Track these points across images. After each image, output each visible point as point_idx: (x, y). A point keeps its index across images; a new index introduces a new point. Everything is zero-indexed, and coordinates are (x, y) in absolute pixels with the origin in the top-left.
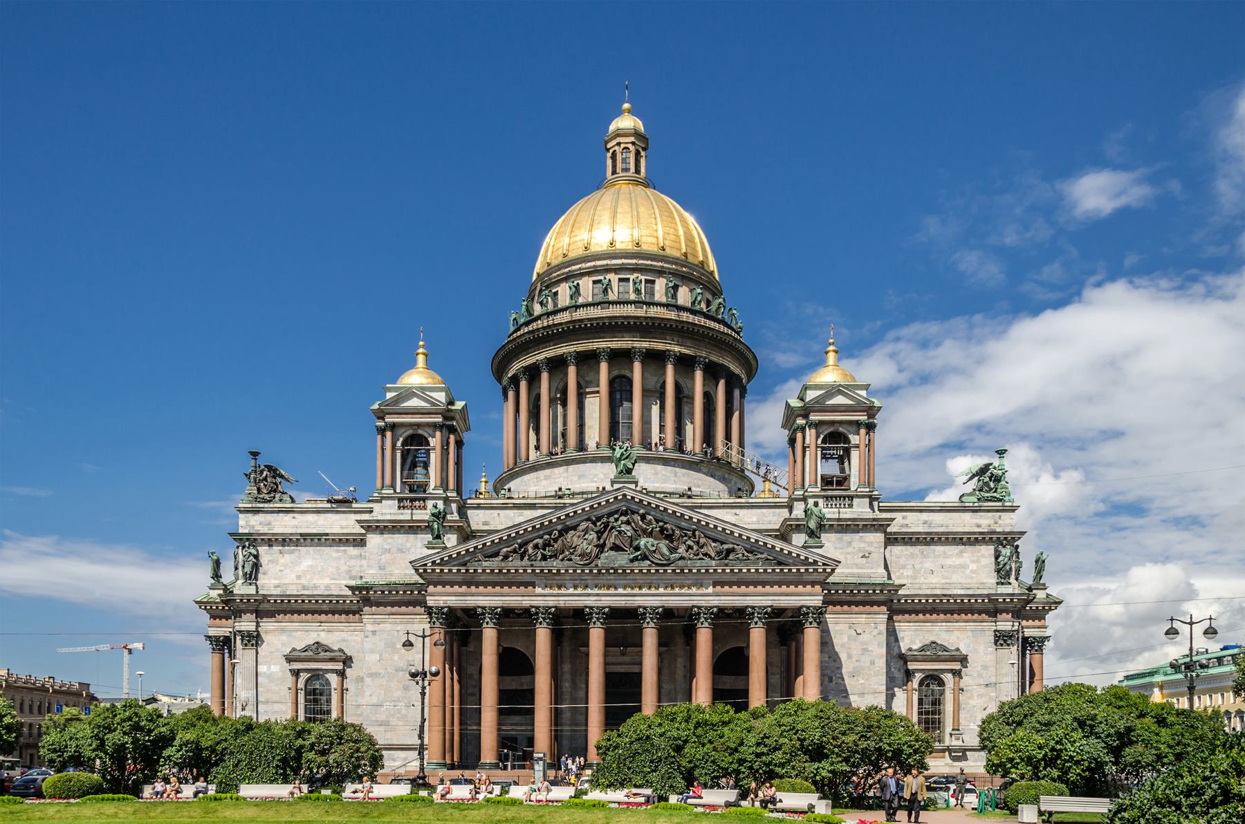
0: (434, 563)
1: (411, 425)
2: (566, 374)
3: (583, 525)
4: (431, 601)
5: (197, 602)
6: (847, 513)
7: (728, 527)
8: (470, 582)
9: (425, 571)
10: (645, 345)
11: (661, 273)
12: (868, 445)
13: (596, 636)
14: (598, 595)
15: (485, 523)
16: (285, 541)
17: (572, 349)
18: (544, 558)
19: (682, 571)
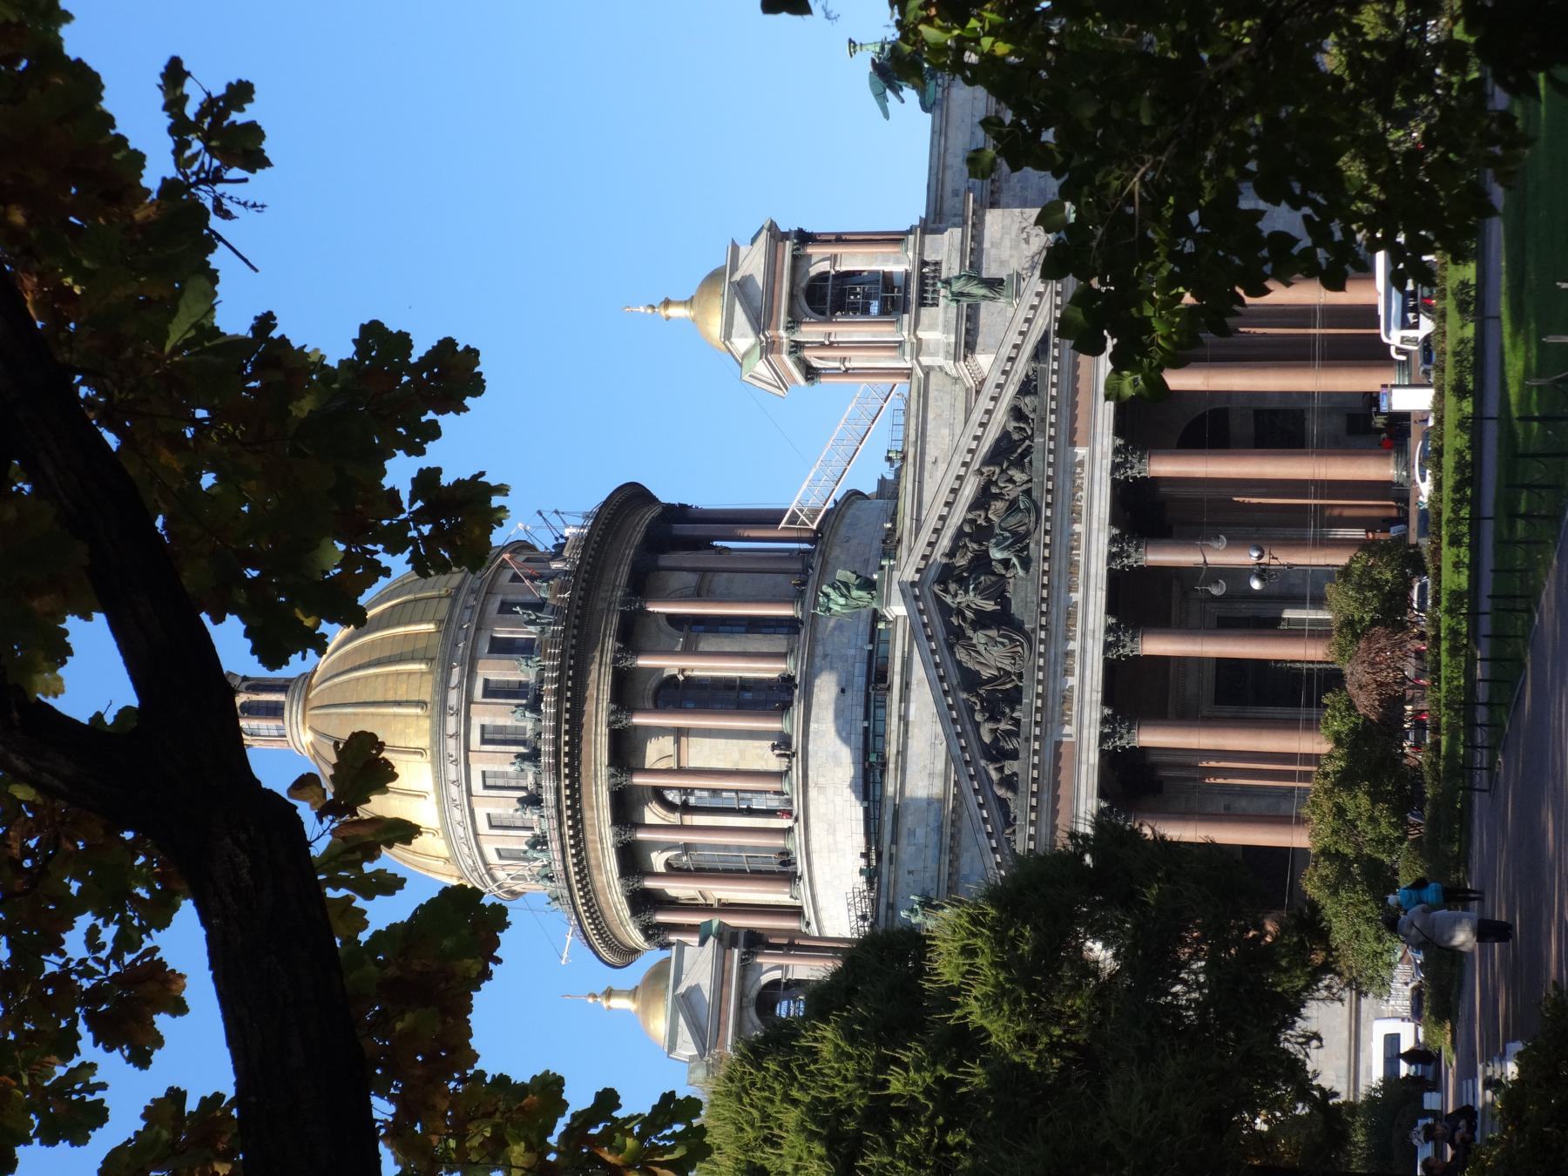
1: (740, 1008)
2: (643, 787)
3: (961, 655)
6: (951, 267)
7: (977, 416)
10: (610, 644)
13: (1155, 646)
14: (1084, 635)
17: (604, 771)
19: (1048, 491)
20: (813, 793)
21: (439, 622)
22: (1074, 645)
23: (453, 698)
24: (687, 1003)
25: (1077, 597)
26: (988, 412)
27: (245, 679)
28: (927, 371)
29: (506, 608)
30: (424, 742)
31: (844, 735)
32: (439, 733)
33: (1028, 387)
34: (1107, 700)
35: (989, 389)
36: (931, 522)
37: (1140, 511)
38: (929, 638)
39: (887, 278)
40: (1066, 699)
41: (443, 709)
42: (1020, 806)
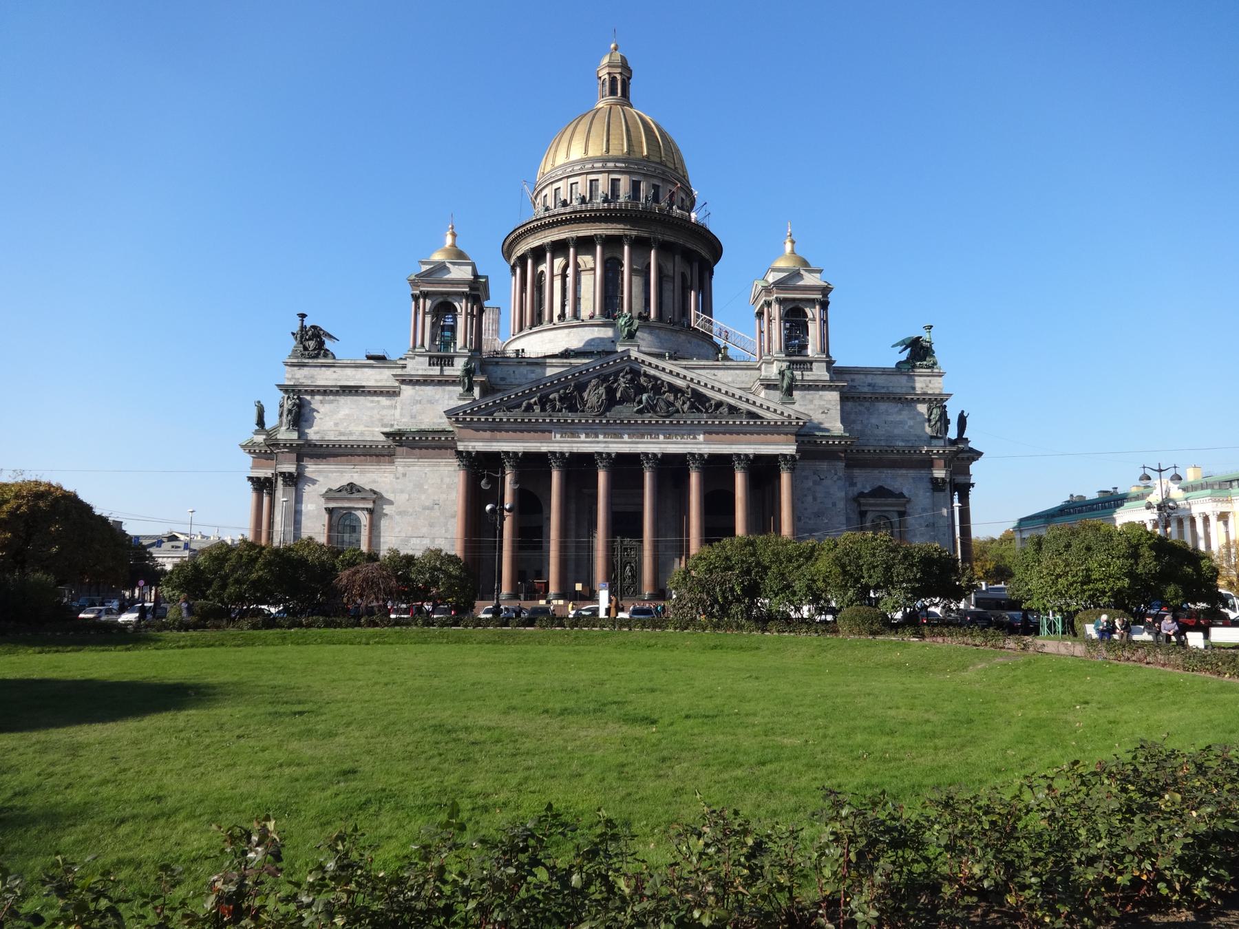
0: (465, 413)
1: (442, 293)
3: (594, 382)
4: (460, 448)
5: (244, 447)
6: (809, 376)
7: (717, 385)
8: (496, 428)
9: (457, 420)
10: (634, 233)
11: (644, 175)
12: (825, 322)
15: (503, 379)
16: (325, 392)
17: (574, 234)
18: (560, 410)
20: (566, 331)
21: (647, 156)
22: (601, 437)
23: (611, 165)
24: (441, 267)
25: (626, 437)
26: (719, 390)
27: (629, 78)
28: (759, 369)
29: (656, 187)
30: (591, 154)
31: (590, 342)
32: (595, 160)
33: (733, 410)
34: (572, 454)
35: (752, 398)
36: (661, 364)
37: (672, 470)
38: (601, 366)
39: (805, 347)
40: (573, 435)
41: (605, 160)
42: (517, 414)
